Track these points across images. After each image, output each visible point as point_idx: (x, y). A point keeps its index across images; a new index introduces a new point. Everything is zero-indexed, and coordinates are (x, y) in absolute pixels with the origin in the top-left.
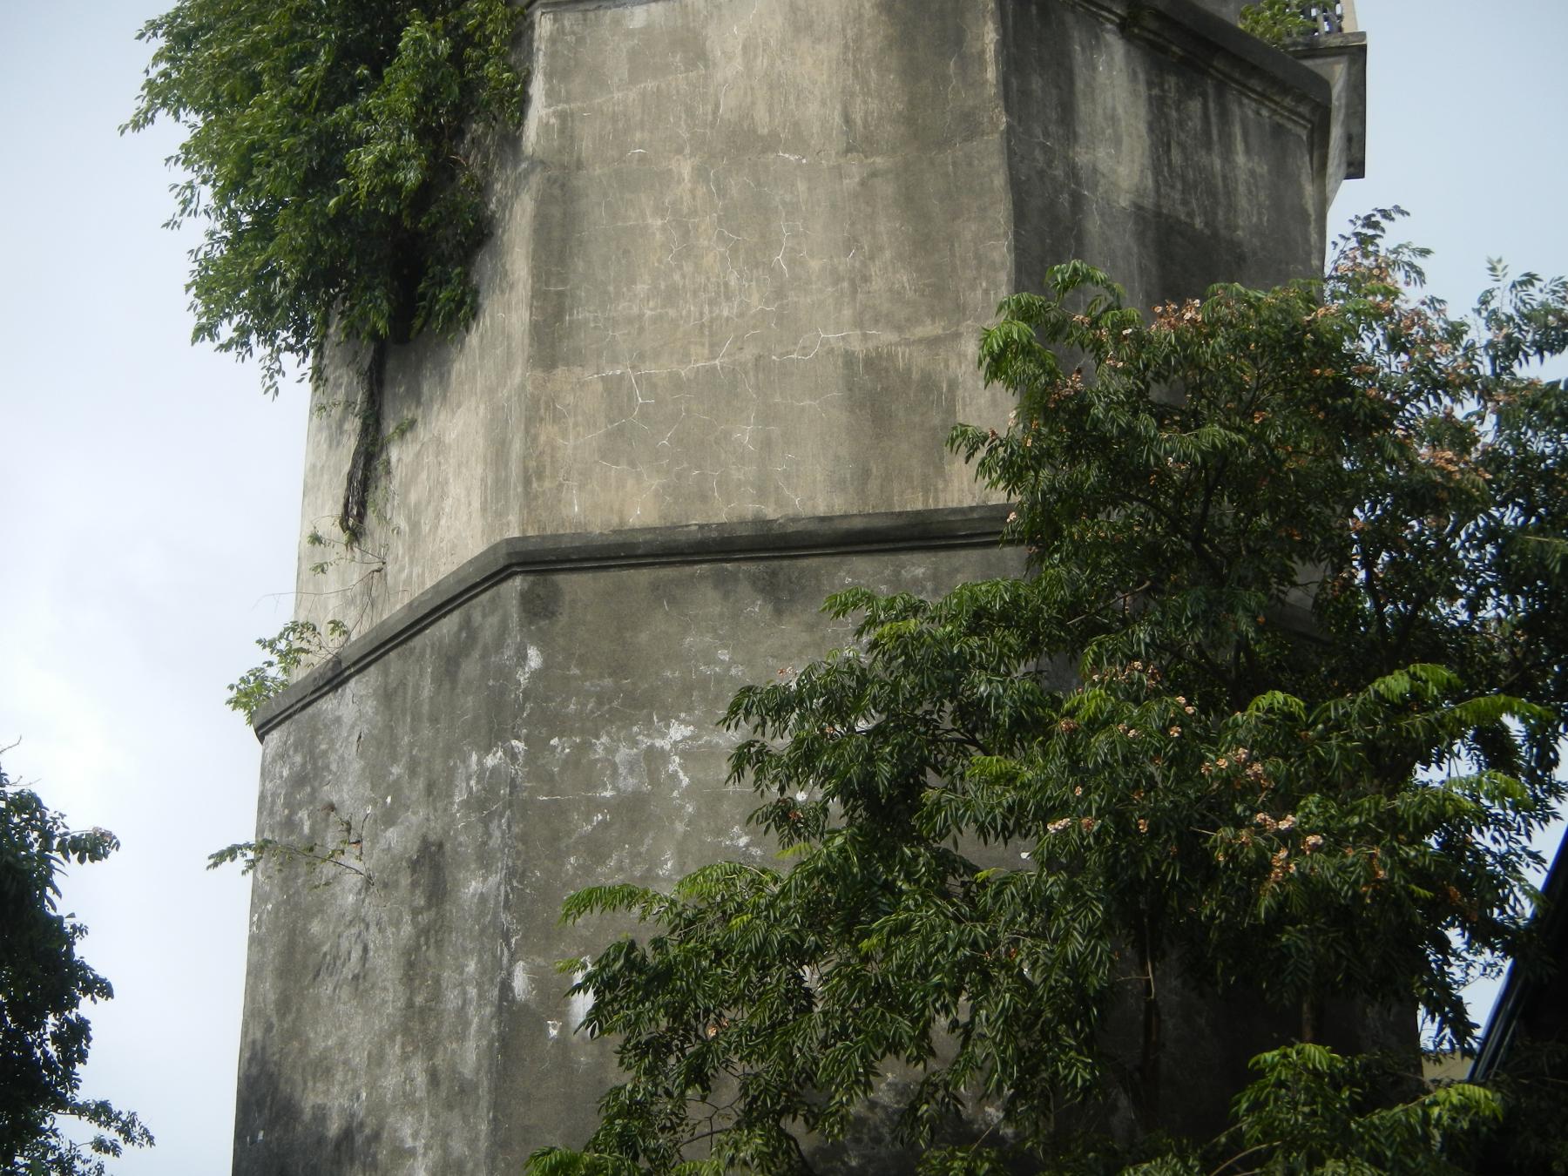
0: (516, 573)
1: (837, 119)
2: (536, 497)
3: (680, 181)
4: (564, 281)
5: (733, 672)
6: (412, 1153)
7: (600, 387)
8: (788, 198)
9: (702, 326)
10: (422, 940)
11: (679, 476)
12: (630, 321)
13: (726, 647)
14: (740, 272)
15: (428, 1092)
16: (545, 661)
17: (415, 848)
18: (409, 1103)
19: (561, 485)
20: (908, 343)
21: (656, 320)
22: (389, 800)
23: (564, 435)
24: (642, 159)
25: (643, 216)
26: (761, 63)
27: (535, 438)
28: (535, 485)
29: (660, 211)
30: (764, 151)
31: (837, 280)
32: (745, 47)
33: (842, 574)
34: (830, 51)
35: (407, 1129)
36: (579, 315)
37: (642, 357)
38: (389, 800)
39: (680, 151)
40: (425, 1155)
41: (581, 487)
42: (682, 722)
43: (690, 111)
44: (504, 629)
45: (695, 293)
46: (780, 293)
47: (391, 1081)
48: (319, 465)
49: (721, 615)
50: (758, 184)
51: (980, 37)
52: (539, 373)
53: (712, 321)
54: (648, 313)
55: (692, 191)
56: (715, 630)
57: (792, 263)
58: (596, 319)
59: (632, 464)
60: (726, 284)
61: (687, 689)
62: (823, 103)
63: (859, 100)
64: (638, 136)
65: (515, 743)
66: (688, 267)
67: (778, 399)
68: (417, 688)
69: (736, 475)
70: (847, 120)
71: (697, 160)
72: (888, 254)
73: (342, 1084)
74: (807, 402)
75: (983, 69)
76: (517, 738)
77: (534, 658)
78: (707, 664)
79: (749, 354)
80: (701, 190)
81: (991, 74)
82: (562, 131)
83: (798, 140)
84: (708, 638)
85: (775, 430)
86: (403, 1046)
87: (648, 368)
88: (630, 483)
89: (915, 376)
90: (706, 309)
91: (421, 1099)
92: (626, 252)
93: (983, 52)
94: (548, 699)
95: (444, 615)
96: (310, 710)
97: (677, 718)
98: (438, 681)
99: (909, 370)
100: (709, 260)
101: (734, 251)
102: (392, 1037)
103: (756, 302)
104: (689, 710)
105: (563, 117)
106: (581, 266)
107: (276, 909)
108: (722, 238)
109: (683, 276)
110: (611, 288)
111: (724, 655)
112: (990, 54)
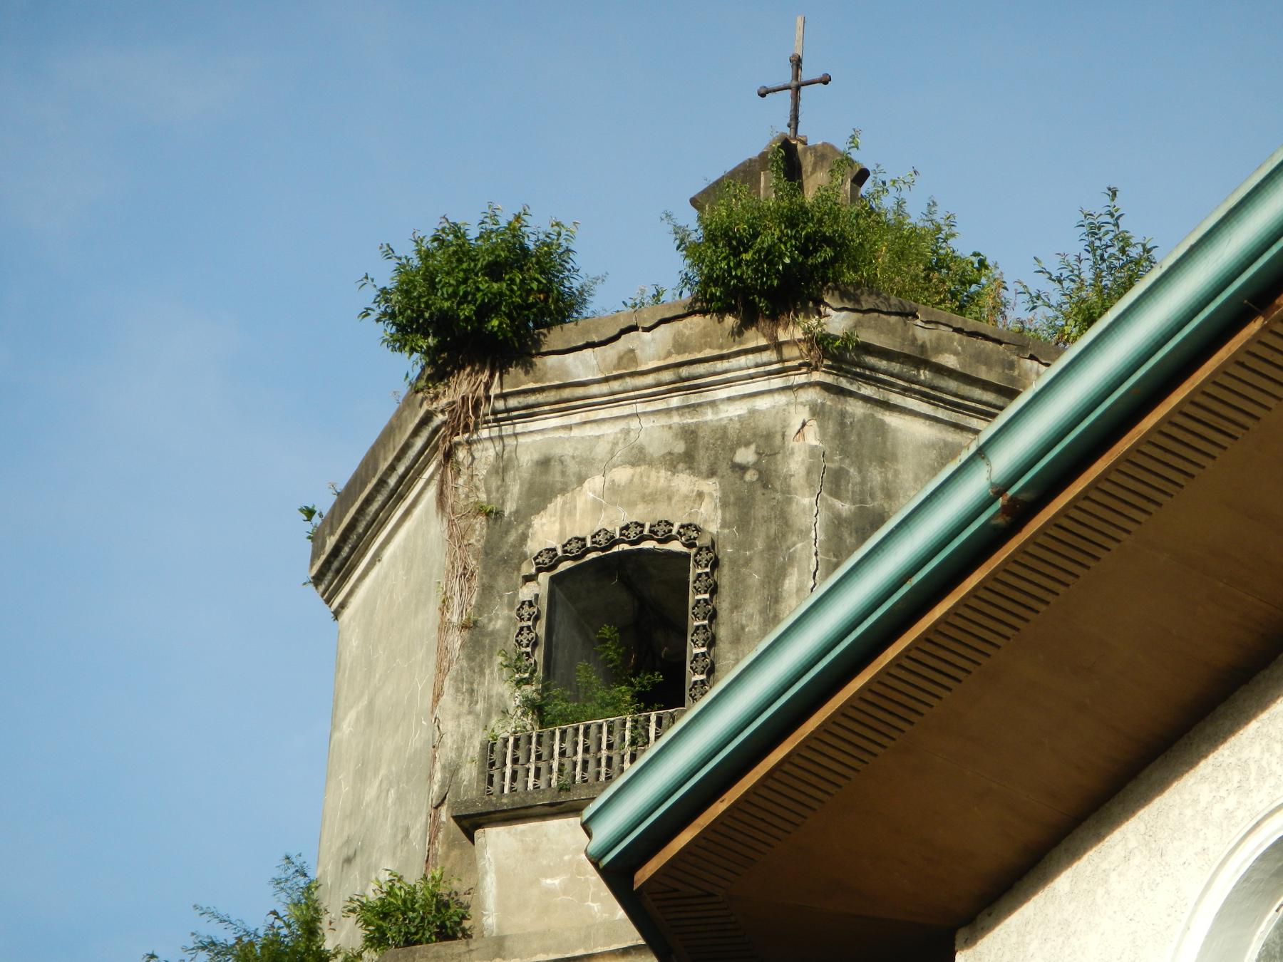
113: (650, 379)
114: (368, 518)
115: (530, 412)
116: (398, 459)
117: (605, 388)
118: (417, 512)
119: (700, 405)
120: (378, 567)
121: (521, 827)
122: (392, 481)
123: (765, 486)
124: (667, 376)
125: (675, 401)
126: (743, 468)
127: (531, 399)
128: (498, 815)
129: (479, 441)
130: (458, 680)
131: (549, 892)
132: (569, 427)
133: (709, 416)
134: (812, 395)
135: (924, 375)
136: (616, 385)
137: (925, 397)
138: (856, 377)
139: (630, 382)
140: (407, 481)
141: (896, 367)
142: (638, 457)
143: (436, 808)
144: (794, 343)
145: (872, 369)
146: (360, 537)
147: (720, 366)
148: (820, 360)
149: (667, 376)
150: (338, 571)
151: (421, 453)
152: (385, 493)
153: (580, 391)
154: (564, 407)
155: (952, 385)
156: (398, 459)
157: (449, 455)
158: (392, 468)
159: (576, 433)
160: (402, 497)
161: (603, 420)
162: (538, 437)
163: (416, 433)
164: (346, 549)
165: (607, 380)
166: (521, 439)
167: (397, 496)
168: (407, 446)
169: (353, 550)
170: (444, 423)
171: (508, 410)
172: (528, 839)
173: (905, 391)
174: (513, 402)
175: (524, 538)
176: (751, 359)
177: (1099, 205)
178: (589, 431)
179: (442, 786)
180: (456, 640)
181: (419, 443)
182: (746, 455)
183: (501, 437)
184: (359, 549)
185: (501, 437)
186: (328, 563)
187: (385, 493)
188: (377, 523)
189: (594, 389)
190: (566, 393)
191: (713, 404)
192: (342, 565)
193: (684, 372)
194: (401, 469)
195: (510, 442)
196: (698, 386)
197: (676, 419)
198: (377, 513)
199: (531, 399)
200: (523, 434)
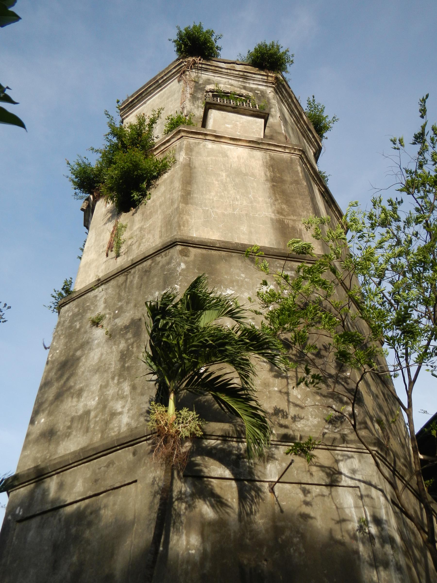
0: (177, 245)
1: (263, 174)
2: (182, 230)
3: (222, 176)
4: (191, 188)
5: (246, 280)
6: (121, 413)
7: (202, 211)
8: (252, 185)
9: (230, 205)
10: (130, 347)
11: (225, 234)
12: (210, 199)
13: (243, 274)
14: (240, 197)
15: (131, 393)
16: (186, 267)
17: (128, 322)
18: (120, 397)
19: (190, 230)
20: (287, 219)
21: (217, 201)
22: (117, 312)
23: (191, 219)
24: (211, 170)
25: (213, 181)
26: (242, 161)
27: (182, 218)
28: (182, 227)
29: (217, 180)
30: (245, 175)
31: (267, 203)
32: (238, 157)
33: (276, 263)
34: (261, 162)
35: (118, 406)
36: (195, 195)
37: (214, 207)
38: (117, 312)
39: (222, 171)
40: (128, 413)
41: (196, 231)
42: (231, 289)
43: (224, 165)
44: (172, 258)
45: (228, 198)
46: (251, 202)
47: (111, 391)
48: (90, 246)
49: (241, 266)
50: (243, 181)
51: (297, 168)
52: (184, 205)
53: (233, 204)
54: (215, 199)
55: (226, 179)
56: (240, 269)
57: (254, 197)
58: (200, 197)
59: (211, 229)
60: (236, 198)
61: (232, 282)
62: (259, 170)
63: (268, 172)
64: (211, 166)
65: (176, 286)
66: (226, 193)
67: (253, 223)
68: (131, 282)
69: (242, 236)
70: (266, 175)
71: (227, 173)
72: (279, 201)
73: (86, 397)
74: (261, 226)
75: (299, 173)
76: (177, 285)
77: (183, 266)
78: (238, 277)
79: (244, 212)
80: (228, 179)
81: (301, 175)
82: (190, 161)
83: (253, 175)
84: (238, 271)
85: (253, 230)
86: (118, 380)
87: (215, 210)
88: (211, 233)
89: (290, 226)
90: (231, 201)
91: (127, 395)
92: (208, 186)
93: (297, 171)
94: (187, 276)
95: (145, 261)
96: (83, 297)
97: (229, 288)
98: (141, 278)
99: (289, 225)
100: (231, 192)
101: (238, 192)
102: (113, 378)
103: (245, 203)
104: (233, 287)
105: (190, 158)
106: (195, 186)
107: (61, 352)
108: (234, 189)
109: (224, 194)
110: (204, 192)
111: (243, 275)
112: (300, 171)
113: (237, 73)
114: (147, 92)
115: (206, 70)
116: (165, 75)
117: (226, 71)
118: (164, 90)
119: (246, 82)
120: (144, 105)
121: (222, 112)
122: (160, 82)
123: (263, 97)
124: (241, 73)
125: (241, 80)
126: (258, 94)
127: (208, 67)
128: (218, 106)
129: (193, 72)
130: (190, 100)
131: (227, 127)
132: (215, 76)
133: (248, 85)
134: (272, 89)
135: (290, 100)
136: (229, 71)
137: (288, 105)
138: (280, 92)
139: (232, 72)
140: (164, 82)
141: (286, 95)
142: (232, 85)
143: (185, 116)
144: (272, 77)
145: (283, 92)
146: (142, 98)
147: (254, 76)
148: (276, 83)
149: (241, 73)
150: (130, 107)
151: (173, 73)
152: (156, 85)
153: (220, 69)
154: (215, 72)
155: (293, 106)
156: (165, 75)
157: (184, 72)
158: (162, 77)
159: (216, 78)
160: (160, 87)
161: (223, 77)
162: (206, 76)
163: (174, 68)
164: (136, 101)
165: (227, 69)
166: (202, 75)
167: (160, 86)
168: (170, 71)
169: (138, 101)
170: (185, 65)
171: (201, 67)
172: (224, 115)
173: (285, 101)
174: (203, 66)
175: (205, 87)
176: (261, 77)
177: (311, 99)
178: (219, 78)
179: (187, 113)
180: (189, 96)
181: (174, 70)
182: (259, 92)
183: (198, 73)
184: (143, 98)
185: (198, 73)
186: (128, 104)
187: (156, 85)
188: (150, 93)
189: (224, 70)
190: (217, 69)
191: (249, 83)
192: (132, 105)
193: (245, 74)
194: (165, 78)
195: (200, 75)
196: (247, 79)
197: (240, 83)
198: (151, 91)
199: (208, 67)
200: (203, 74)
